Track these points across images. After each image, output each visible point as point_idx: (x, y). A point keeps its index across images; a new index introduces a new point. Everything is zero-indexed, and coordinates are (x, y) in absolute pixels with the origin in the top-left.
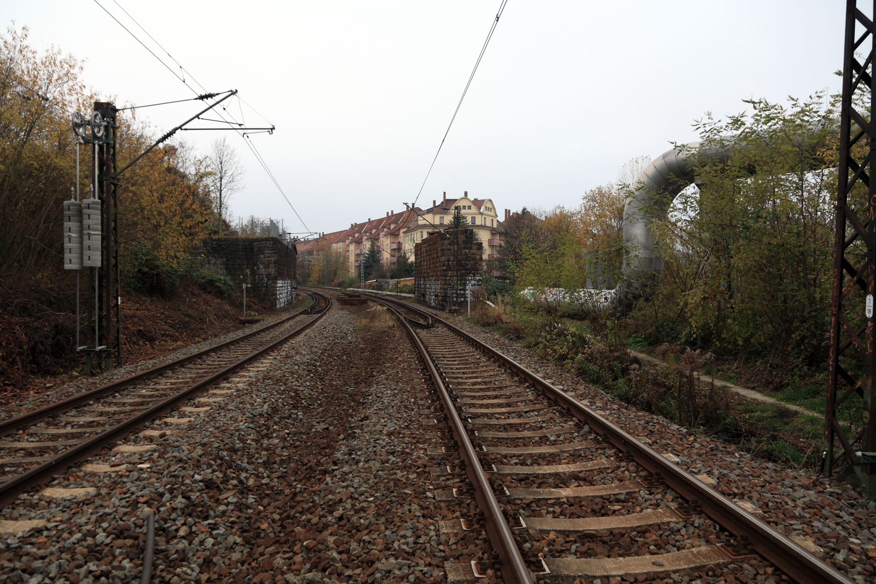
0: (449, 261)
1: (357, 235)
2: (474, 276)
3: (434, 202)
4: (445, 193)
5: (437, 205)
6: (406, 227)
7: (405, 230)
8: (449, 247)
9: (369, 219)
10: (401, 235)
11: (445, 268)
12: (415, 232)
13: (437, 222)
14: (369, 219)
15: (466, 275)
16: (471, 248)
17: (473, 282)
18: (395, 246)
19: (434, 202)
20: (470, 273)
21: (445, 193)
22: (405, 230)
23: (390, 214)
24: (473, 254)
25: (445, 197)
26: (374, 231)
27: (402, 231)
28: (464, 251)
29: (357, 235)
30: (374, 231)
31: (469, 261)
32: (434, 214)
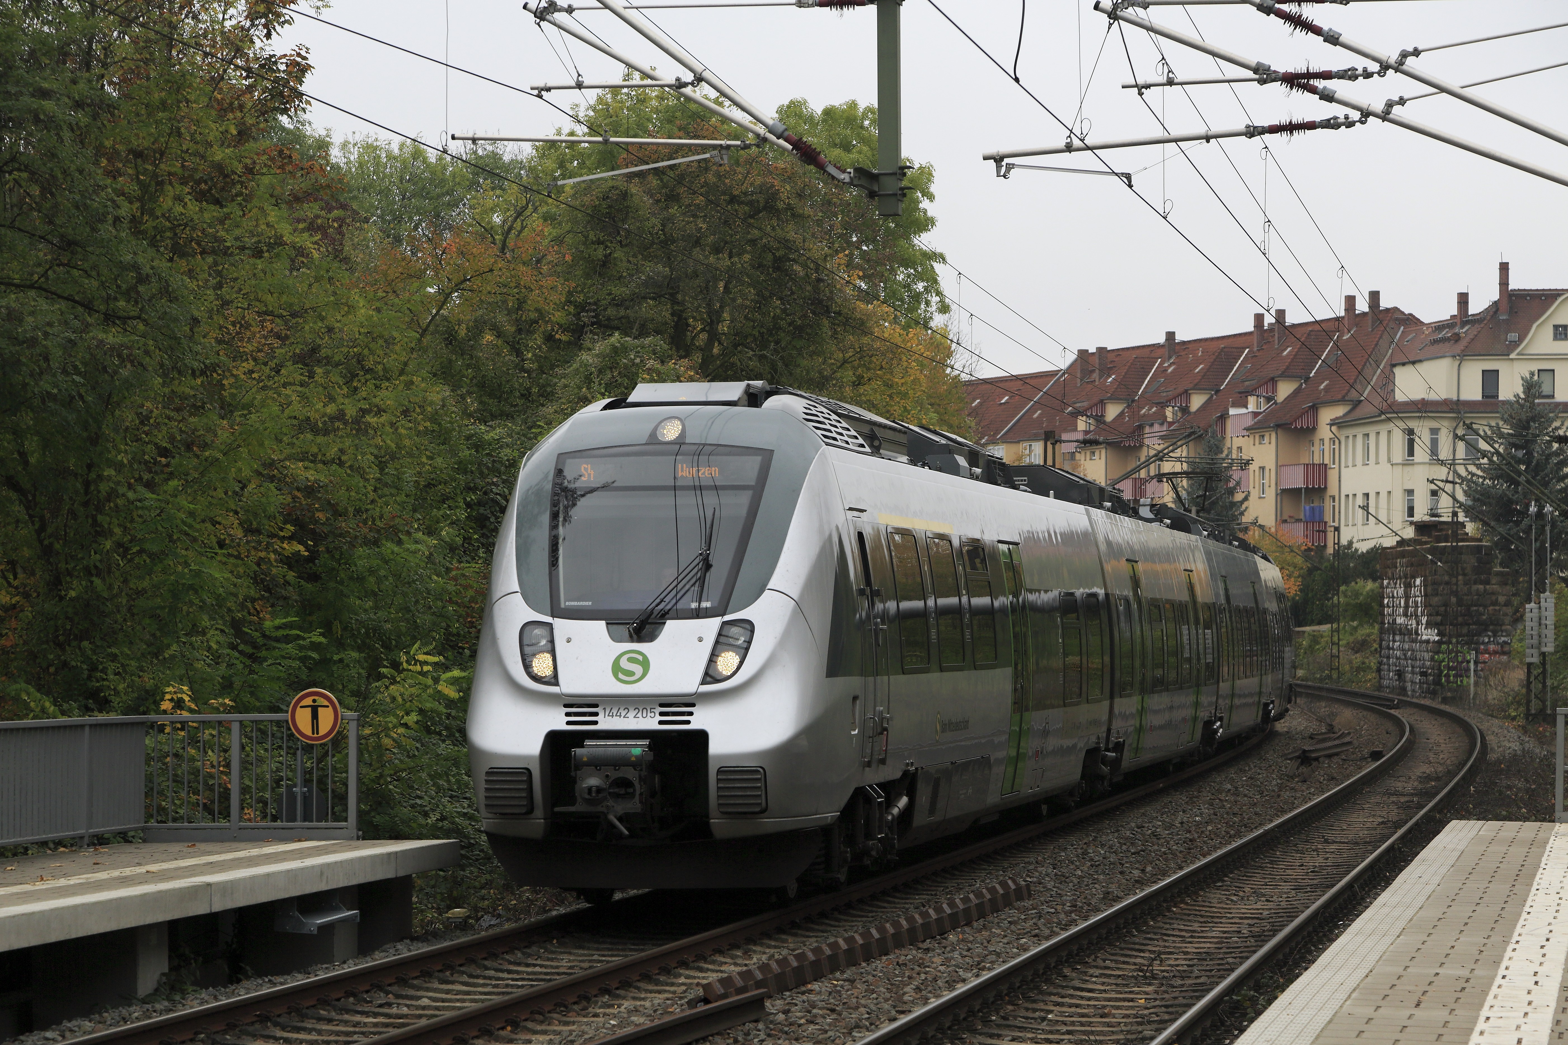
0: (1446, 605)
1: (1112, 412)
2: (1495, 636)
3: (1463, 299)
4: (1504, 268)
5: (1476, 307)
6: (1342, 401)
7: (1339, 411)
8: (1446, 578)
9: (1170, 335)
10: (1324, 432)
11: (1439, 618)
12: (1383, 429)
13: (1473, 391)
14: (1170, 335)
15: (1479, 634)
16: (1487, 582)
17: (1492, 647)
18: (1296, 479)
19: (1463, 299)
20: (1486, 630)
21: (1504, 268)
22: (1339, 411)
23: (1269, 320)
24: (1493, 593)
25: (1504, 282)
26: (1197, 402)
27: (1327, 415)
28: (1475, 587)
29: (1112, 412)
30: (1197, 402)
31: (1485, 607)
32: (1463, 356)
